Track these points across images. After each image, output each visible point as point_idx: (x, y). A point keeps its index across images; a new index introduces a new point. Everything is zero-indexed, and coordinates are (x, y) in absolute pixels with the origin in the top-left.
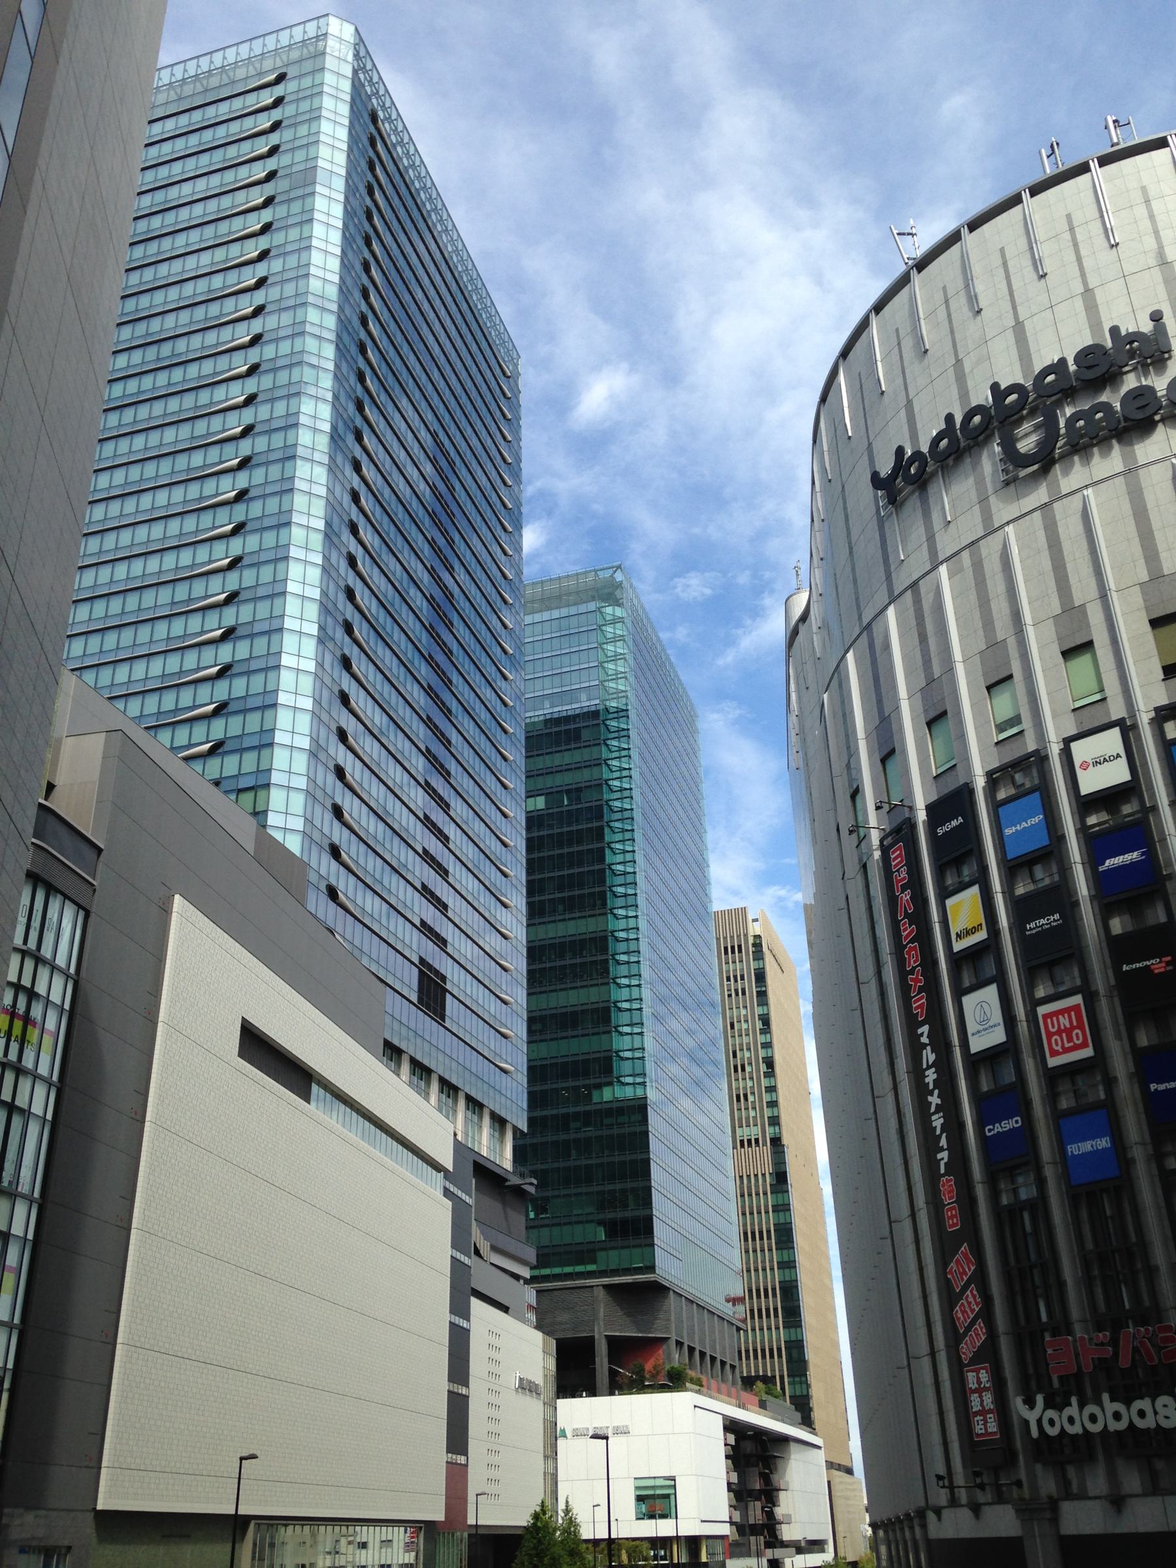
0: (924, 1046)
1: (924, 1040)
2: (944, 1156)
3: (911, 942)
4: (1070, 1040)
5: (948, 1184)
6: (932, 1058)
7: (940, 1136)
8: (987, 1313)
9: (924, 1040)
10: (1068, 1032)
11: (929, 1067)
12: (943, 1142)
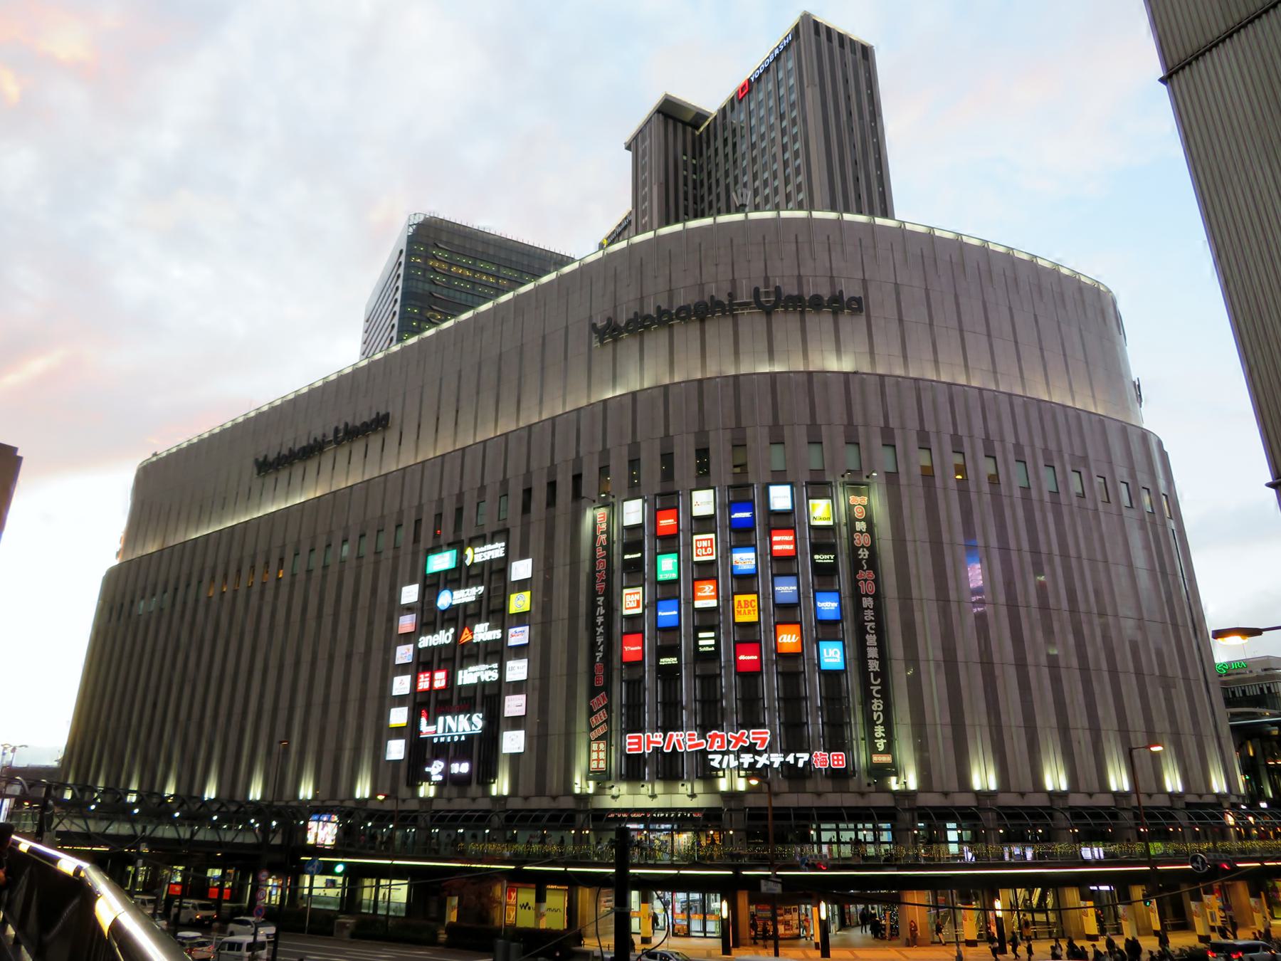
0: (600, 606)
1: (600, 603)
2: (600, 655)
3: (603, 558)
4: (706, 551)
5: (599, 665)
7: (599, 646)
8: (608, 721)
9: (600, 603)
10: (706, 548)
11: (600, 615)
12: (601, 648)
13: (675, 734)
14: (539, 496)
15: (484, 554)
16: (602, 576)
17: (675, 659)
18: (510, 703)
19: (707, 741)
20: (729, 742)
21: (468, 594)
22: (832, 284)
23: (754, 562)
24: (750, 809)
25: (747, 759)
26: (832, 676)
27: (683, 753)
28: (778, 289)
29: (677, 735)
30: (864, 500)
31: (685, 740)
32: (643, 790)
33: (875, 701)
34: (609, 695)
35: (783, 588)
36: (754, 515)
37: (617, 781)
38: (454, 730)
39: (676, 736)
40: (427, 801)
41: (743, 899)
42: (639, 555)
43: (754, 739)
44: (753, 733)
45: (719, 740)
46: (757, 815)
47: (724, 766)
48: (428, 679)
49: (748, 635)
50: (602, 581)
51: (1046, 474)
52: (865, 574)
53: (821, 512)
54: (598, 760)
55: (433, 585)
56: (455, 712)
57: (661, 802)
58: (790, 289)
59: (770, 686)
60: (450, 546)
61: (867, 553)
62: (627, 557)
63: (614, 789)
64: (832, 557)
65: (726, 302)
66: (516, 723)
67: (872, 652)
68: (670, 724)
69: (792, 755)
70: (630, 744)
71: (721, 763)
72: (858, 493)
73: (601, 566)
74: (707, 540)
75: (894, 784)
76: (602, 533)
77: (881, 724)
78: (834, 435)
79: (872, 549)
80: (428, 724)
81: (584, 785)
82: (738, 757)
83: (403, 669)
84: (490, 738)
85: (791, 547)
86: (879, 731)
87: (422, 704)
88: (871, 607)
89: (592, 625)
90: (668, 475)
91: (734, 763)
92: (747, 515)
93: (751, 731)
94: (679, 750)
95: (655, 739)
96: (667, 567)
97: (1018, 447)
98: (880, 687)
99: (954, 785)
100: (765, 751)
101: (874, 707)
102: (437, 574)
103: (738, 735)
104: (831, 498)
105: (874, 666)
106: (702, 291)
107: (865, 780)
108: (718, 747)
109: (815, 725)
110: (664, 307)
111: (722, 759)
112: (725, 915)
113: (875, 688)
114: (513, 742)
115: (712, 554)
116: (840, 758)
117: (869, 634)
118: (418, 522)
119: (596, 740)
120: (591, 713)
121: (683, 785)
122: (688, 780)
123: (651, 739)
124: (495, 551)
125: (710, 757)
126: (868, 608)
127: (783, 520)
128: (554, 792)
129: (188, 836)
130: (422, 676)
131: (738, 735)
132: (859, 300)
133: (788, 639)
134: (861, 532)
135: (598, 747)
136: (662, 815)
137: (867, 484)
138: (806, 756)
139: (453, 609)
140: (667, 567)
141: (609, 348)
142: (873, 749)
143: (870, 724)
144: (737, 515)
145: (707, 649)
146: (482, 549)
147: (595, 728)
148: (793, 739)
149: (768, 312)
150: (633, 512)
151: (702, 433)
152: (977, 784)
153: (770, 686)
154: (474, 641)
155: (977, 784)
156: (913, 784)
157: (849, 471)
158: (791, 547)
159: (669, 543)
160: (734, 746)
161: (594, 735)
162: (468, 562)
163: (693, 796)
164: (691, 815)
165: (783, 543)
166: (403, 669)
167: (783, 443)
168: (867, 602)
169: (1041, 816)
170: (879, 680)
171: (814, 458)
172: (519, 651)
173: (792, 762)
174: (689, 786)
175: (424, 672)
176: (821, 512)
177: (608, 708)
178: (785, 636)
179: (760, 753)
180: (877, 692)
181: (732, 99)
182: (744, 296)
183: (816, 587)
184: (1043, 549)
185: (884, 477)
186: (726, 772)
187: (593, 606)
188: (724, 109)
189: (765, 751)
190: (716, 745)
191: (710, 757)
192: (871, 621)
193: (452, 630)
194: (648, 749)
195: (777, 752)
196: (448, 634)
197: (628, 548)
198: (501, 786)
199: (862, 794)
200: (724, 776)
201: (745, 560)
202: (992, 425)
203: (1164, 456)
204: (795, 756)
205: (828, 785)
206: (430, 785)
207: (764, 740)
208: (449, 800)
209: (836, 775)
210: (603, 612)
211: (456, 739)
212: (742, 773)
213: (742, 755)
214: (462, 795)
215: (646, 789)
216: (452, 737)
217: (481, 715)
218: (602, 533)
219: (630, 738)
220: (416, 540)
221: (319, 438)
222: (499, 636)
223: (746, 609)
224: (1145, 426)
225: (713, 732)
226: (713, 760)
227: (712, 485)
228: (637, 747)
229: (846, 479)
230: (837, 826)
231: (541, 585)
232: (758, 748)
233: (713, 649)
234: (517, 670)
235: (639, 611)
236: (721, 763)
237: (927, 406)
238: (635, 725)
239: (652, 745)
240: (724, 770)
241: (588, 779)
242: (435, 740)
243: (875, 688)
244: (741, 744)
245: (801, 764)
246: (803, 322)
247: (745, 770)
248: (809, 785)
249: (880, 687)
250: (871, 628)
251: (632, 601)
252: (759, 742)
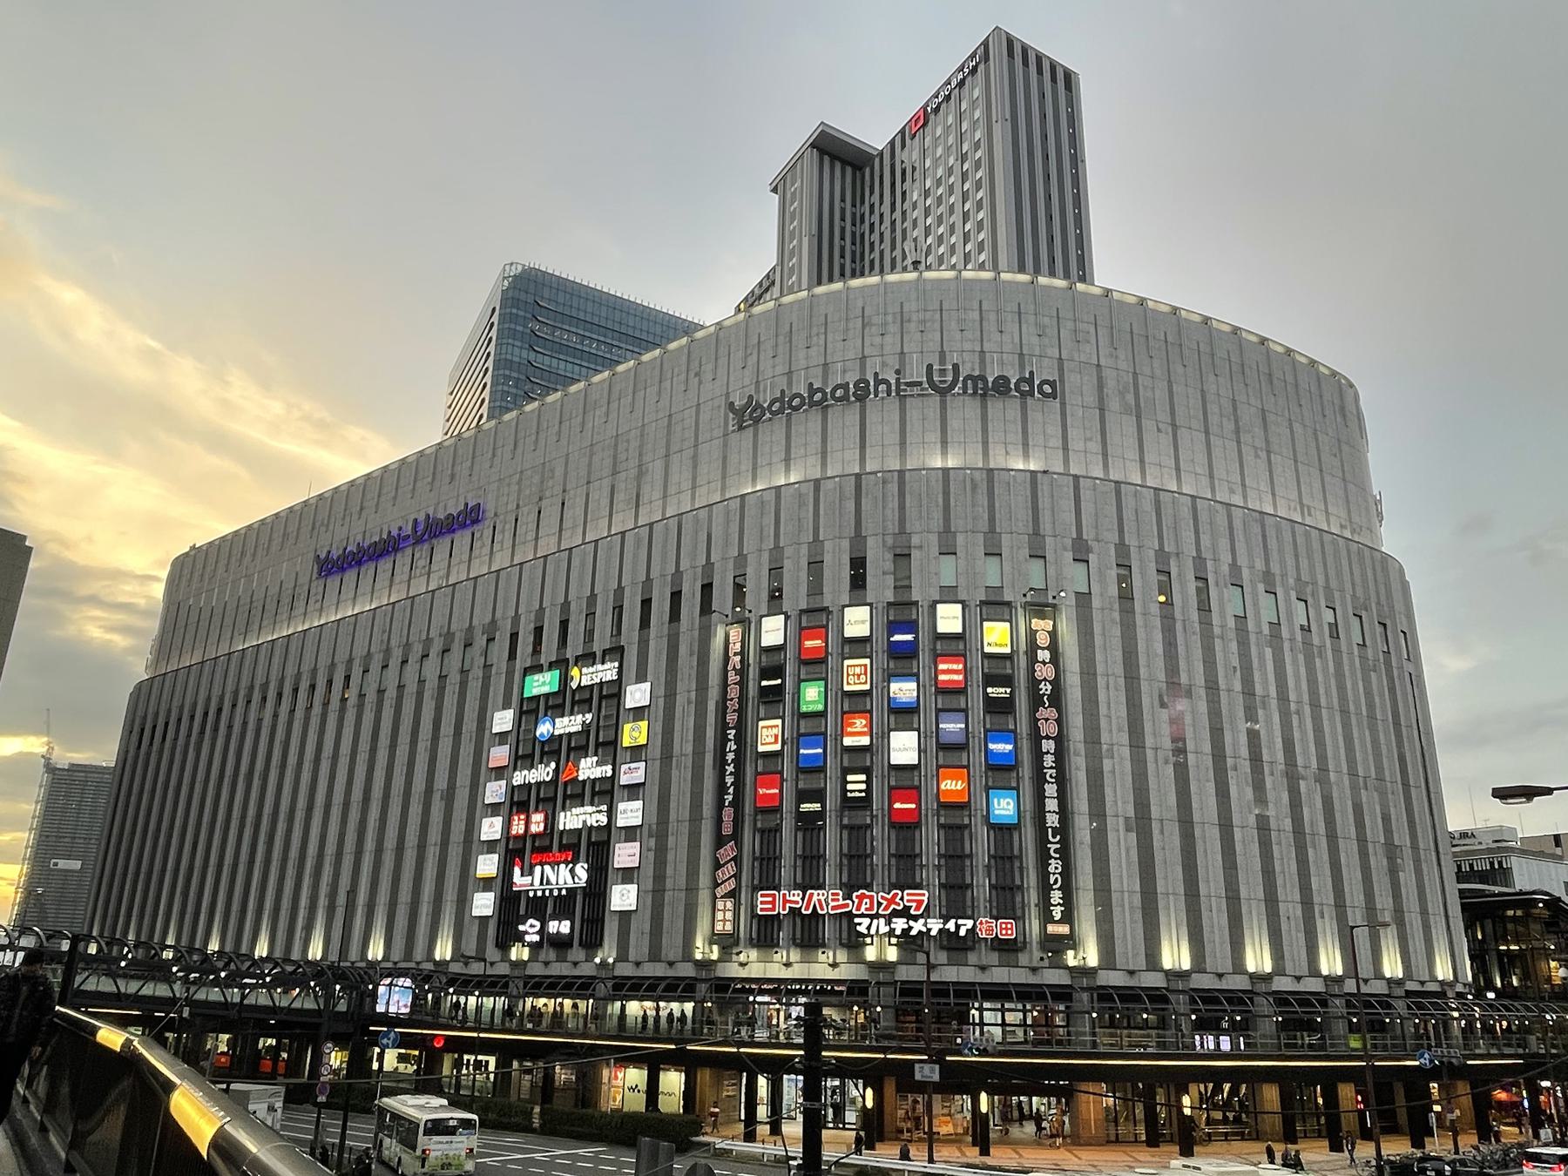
0: (730, 740)
1: (731, 737)
2: (730, 798)
3: (735, 684)
4: (859, 679)
5: (728, 814)
6: (734, 747)
8: (737, 876)
9: (731, 737)
10: (859, 676)
11: (730, 751)
12: (731, 790)
13: (815, 892)
14: (660, 608)
15: (594, 676)
16: (734, 705)
17: (819, 805)
18: (620, 852)
19: (853, 902)
20: (879, 904)
21: (572, 722)
22: (1022, 367)
23: (915, 694)
24: (903, 982)
25: (900, 924)
26: (1003, 831)
27: (824, 915)
29: (818, 895)
30: (1048, 625)
31: (826, 900)
32: (777, 957)
33: (1052, 861)
34: (739, 846)
35: (948, 726)
36: (916, 638)
37: (745, 947)
38: (553, 880)
39: (817, 896)
40: (520, 964)
41: (890, 1088)
42: (779, 681)
43: (908, 901)
44: (908, 894)
45: (868, 900)
46: (910, 990)
47: (873, 931)
48: (523, 822)
49: (905, 780)
50: (734, 711)
51: (1266, 601)
53: (997, 637)
54: (724, 920)
55: (531, 710)
56: (555, 864)
57: (796, 972)
59: (930, 841)
60: (551, 666)
61: (1049, 687)
62: (764, 683)
63: (741, 955)
64: (1008, 690)
65: (893, 382)
66: (627, 875)
67: (1052, 805)
68: (811, 881)
69: (953, 921)
70: (762, 903)
71: (869, 928)
72: (1043, 617)
73: (733, 692)
74: (861, 666)
75: (1071, 959)
76: (735, 654)
77: (1059, 889)
78: (1014, 544)
79: (1056, 683)
80: (522, 875)
81: (707, 950)
82: (889, 923)
83: (494, 809)
84: (596, 892)
85: (960, 677)
86: (1056, 897)
87: (514, 851)
88: (1052, 751)
89: (721, 762)
90: (816, 589)
91: (884, 929)
92: (909, 637)
93: (906, 892)
94: (820, 912)
95: (792, 898)
96: (812, 695)
97: (1235, 567)
98: (1058, 846)
99: (1141, 963)
100: (921, 916)
101: (1051, 869)
102: (537, 698)
103: (889, 897)
104: (1010, 621)
105: (1052, 820)
107: (1037, 954)
108: (866, 909)
109: (982, 886)
111: (870, 925)
112: (869, 1104)
113: (1053, 847)
114: (623, 897)
115: (866, 682)
116: (1009, 926)
117: (1049, 782)
118: (514, 637)
119: (722, 897)
120: (717, 865)
121: (823, 953)
122: (829, 948)
123: (788, 898)
124: (606, 672)
125: (857, 920)
126: (1048, 753)
127: (955, 645)
128: (671, 958)
129: (237, 999)
130: (516, 818)
131: (889, 897)
133: (952, 785)
134: (1044, 663)
135: (725, 906)
136: (798, 987)
137: (1054, 606)
138: (970, 923)
139: (555, 739)
140: (812, 695)
141: (749, 433)
142: (1047, 918)
143: (1045, 889)
144: (897, 638)
145: (857, 794)
146: (591, 669)
147: (723, 882)
148: (955, 900)
150: (773, 631)
151: (858, 539)
152: (1167, 963)
153: (930, 841)
154: (580, 778)
155: (1167, 963)
156: (1093, 960)
157: (1031, 589)
158: (960, 677)
159: (814, 665)
160: (885, 909)
161: (720, 891)
162: (574, 685)
163: (834, 965)
164: (832, 987)
165: (950, 672)
166: (494, 809)
167: (955, 554)
168: (1050, 746)
169: (1241, 1002)
170: (1058, 837)
171: (991, 574)
172: (633, 791)
173: (953, 929)
174: (831, 954)
175: (518, 813)
176: (997, 637)
177: (737, 860)
178: (949, 782)
179: (915, 918)
180: (1055, 851)
181: (902, 132)
183: (988, 726)
184: (1259, 690)
185: (1073, 596)
186: (875, 939)
187: (722, 740)
188: (892, 143)
189: (921, 916)
190: (863, 907)
191: (857, 920)
192: (1051, 768)
193: (553, 765)
194: (784, 909)
195: (935, 917)
196: (548, 769)
197: (766, 673)
198: (607, 953)
199: (1034, 970)
200: (872, 944)
201: (904, 690)
202: (1205, 540)
203: (1405, 587)
204: (956, 923)
205: (994, 958)
206: (523, 946)
207: (920, 903)
208: (546, 964)
209: (1007, 949)
210: (734, 747)
211: (556, 893)
212: (894, 941)
213: (894, 920)
214: (561, 959)
215: (780, 956)
216: (551, 891)
217: (586, 866)
218: (735, 654)
219: (762, 896)
220: (512, 655)
221: (395, 533)
222: (609, 774)
223: (904, 747)
224: (1383, 549)
225: (861, 891)
226: (860, 924)
227: (868, 601)
228: (770, 906)
229: (1028, 599)
230: (1003, 1005)
231: (664, 712)
232: (912, 912)
233: (863, 794)
234: (630, 813)
235: (778, 747)
236: (869, 928)
237: (1128, 514)
238: (769, 881)
239: (788, 905)
240: (872, 936)
241: (711, 944)
242: (531, 894)
243: (1053, 847)
244: (893, 906)
245: (962, 932)
246: (984, 408)
247: (897, 937)
248: (972, 958)
249: (1058, 846)
250: (1051, 776)
251: (769, 735)
252: (914, 905)
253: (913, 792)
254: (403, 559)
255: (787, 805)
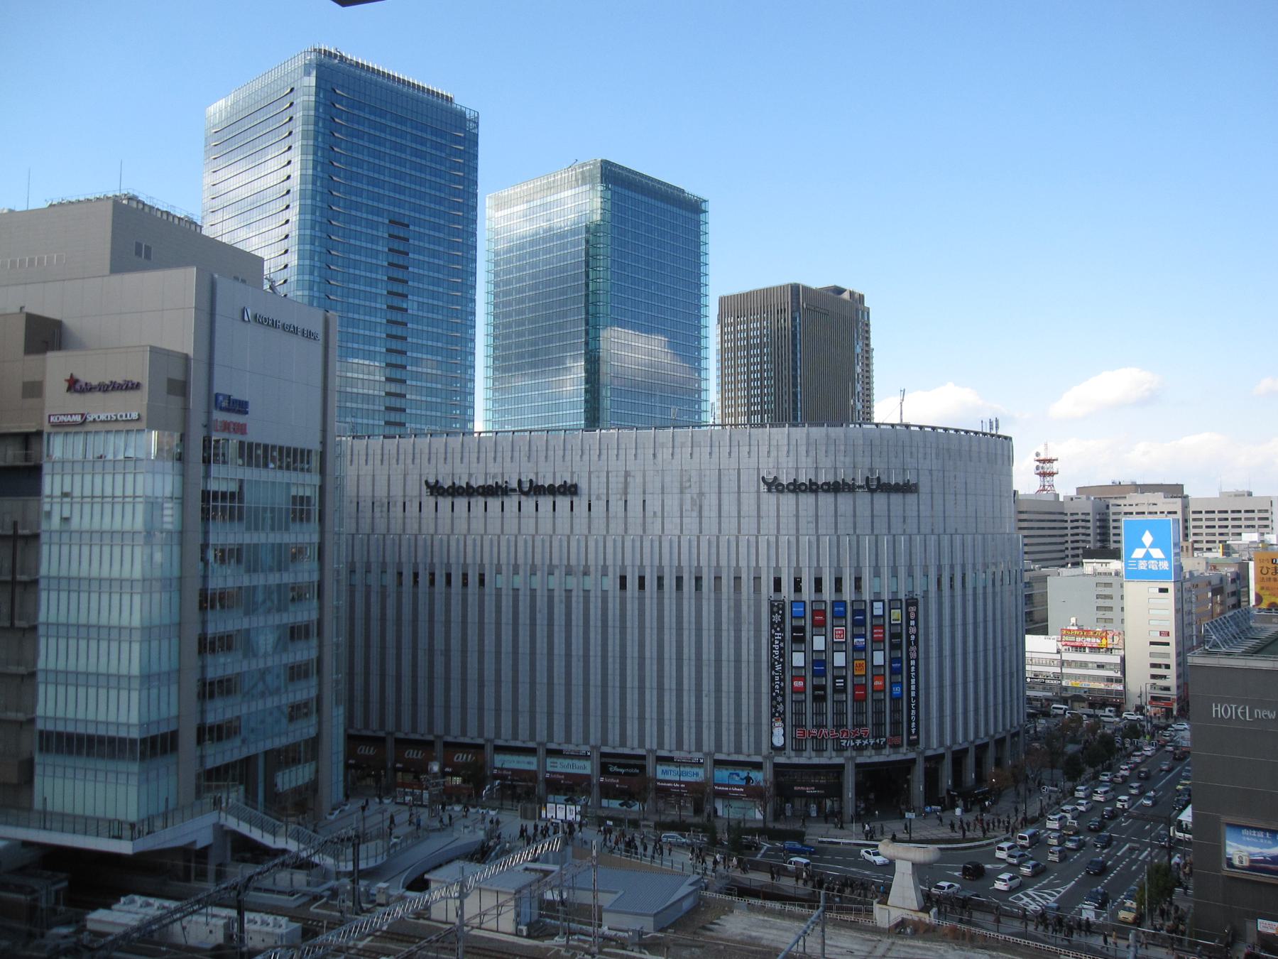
25: (858, 742)
28: (879, 479)
52: (913, 648)
58: (884, 480)
67: (913, 688)
79: (916, 635)
86: (913, 724)
91: (852, 744)
105: (913, 694)
106: (836, 474)
110: (814, 480)
132: (916, 485)
149: (872, 491)
168: (913, 663)
182: (860, 482)
246: (889, 498)
248: (884, 752)
253: (864, 687)
254: (511, 502)
255: (809, 691)
